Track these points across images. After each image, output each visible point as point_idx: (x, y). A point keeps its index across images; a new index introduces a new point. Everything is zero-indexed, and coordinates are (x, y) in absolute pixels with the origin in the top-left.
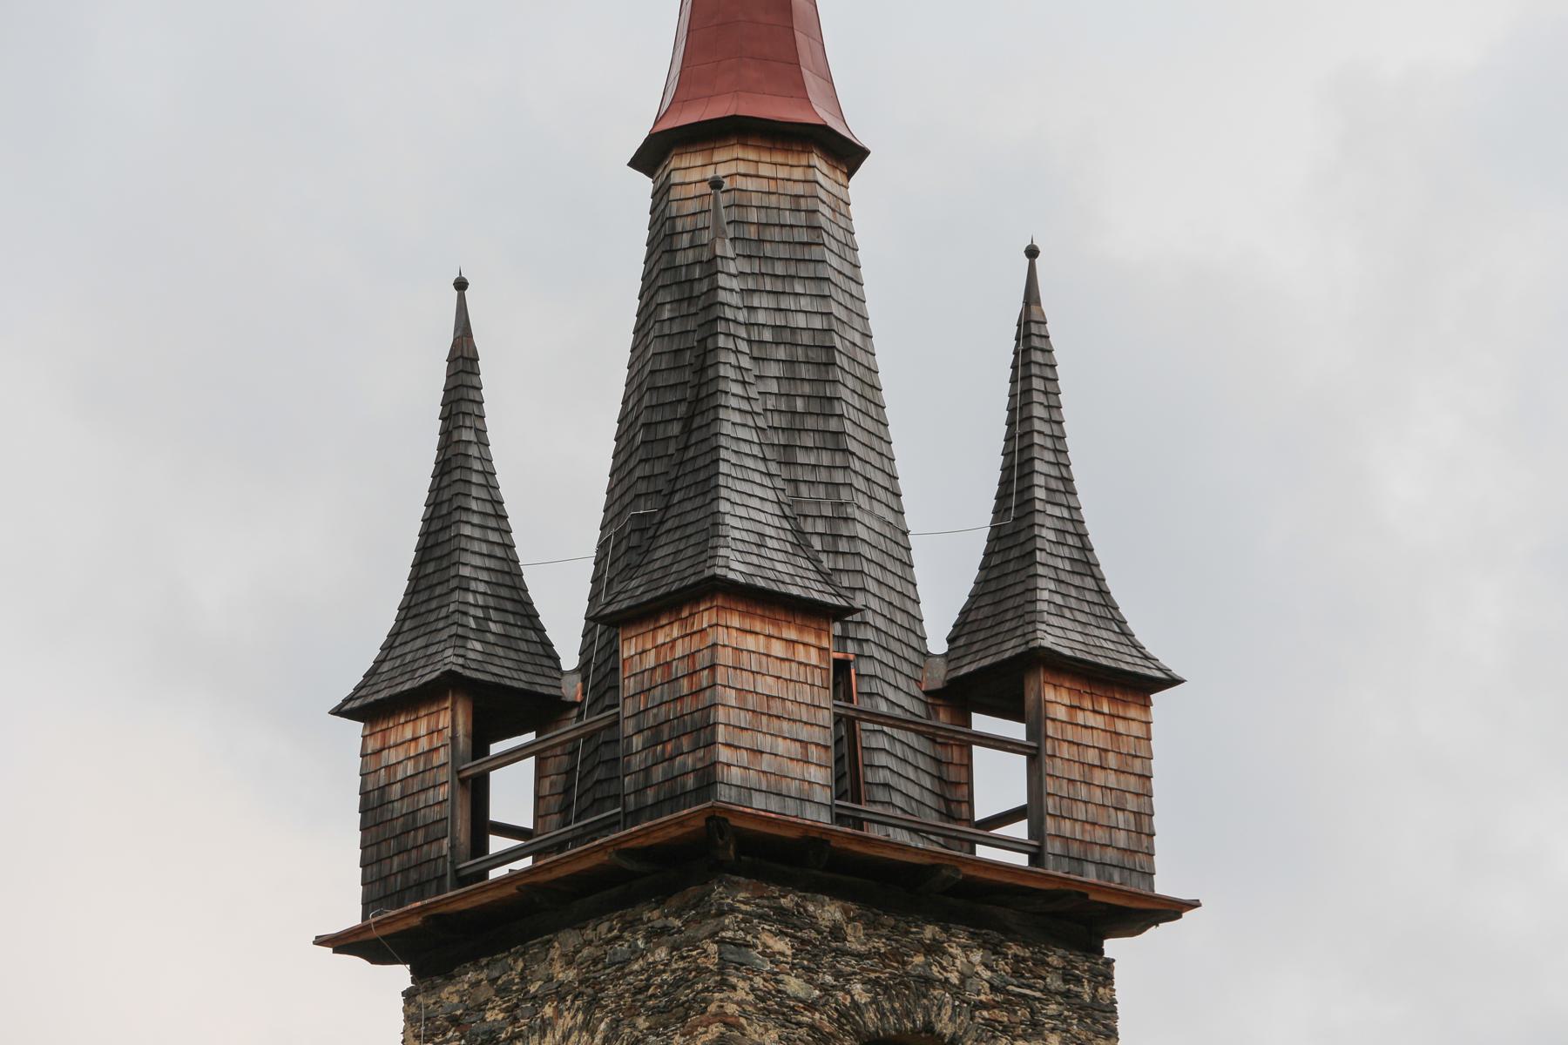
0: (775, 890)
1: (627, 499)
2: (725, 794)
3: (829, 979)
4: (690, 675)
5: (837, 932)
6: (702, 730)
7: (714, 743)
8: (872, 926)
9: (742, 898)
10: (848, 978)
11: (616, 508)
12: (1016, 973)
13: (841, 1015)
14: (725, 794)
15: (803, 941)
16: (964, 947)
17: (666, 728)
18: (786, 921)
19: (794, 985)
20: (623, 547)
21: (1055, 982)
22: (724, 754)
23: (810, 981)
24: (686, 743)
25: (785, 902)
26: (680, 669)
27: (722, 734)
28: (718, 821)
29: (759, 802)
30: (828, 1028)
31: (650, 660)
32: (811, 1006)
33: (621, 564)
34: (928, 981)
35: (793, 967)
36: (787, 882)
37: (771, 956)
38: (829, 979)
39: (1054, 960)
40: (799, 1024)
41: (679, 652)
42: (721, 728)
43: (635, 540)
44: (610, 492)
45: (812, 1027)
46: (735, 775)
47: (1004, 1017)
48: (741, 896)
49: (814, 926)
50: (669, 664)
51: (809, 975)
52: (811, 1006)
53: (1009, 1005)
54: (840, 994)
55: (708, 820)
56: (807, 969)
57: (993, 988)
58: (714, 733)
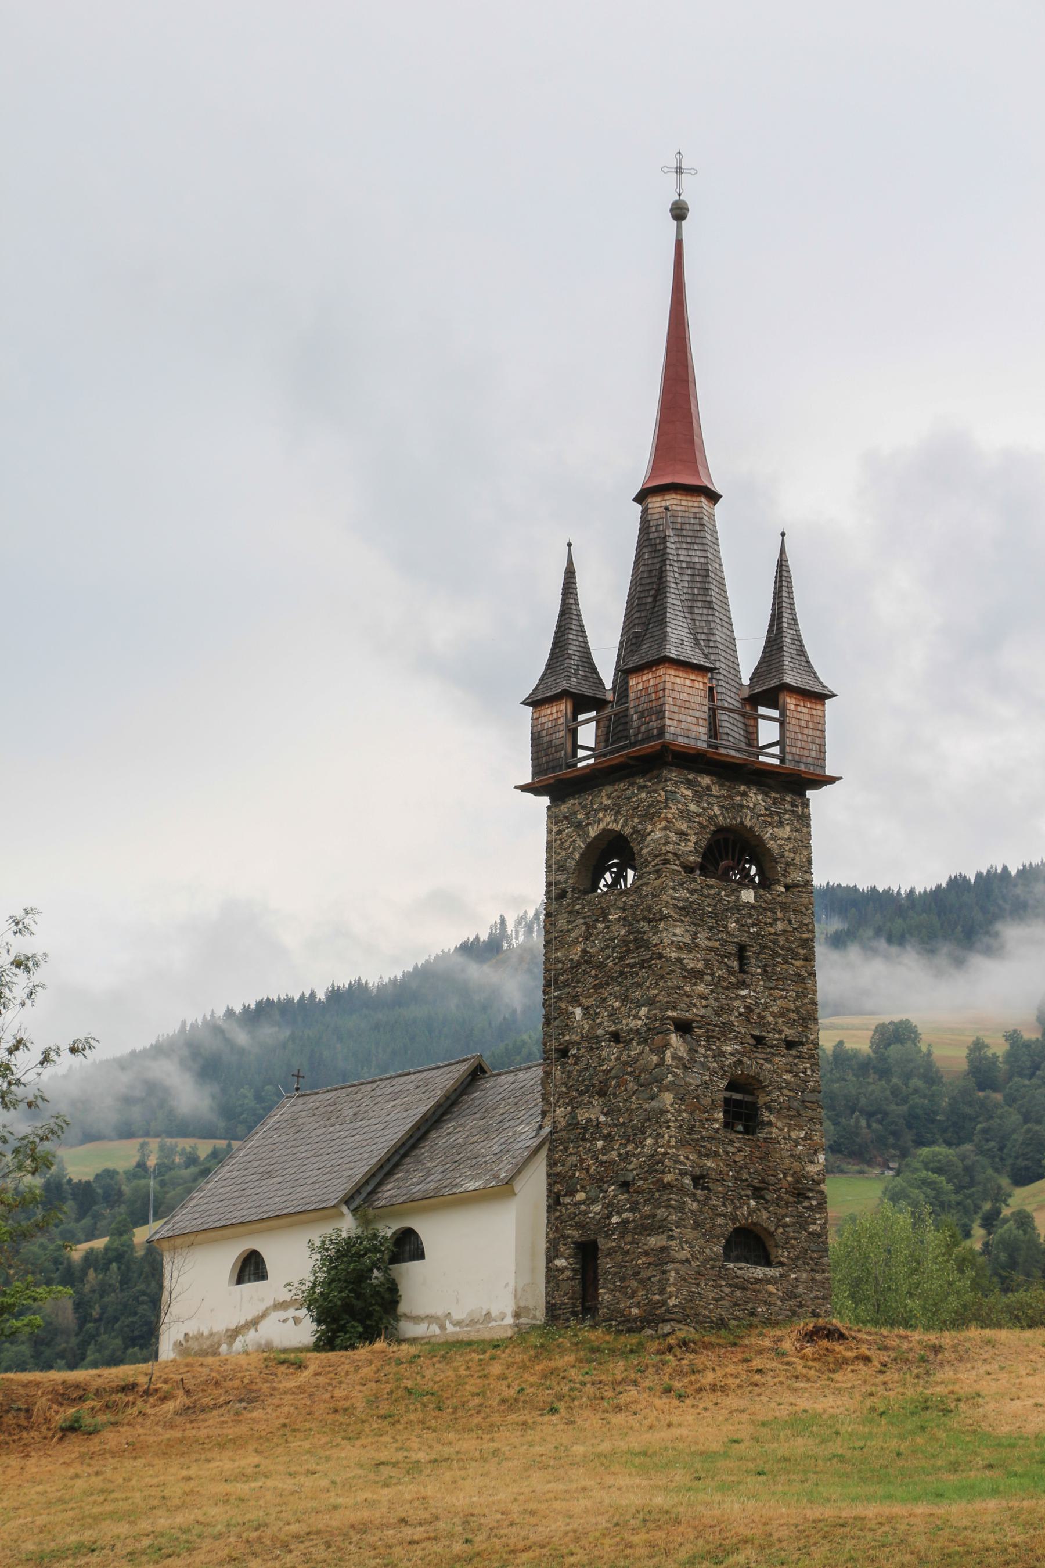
0: (686, 772)
1: (631, 626)
2: (668, 737)
3: (705, 805)
4: (656, 692)
6: (660, 713)
7: (664, 718)
9: (674, 775)
11: (626, 629)
13: (710, 818)
14: (668, 737)
15: (696, 791)
17: (646, 712)
18: (690, 783)
19: (693, 807)
20: (629, 643)
22: (668, 722)
23: (698, 806)
24: (653, 718)
25: (690, 777)
26: (651, 690)
27: (667, 714)
28: (666, 747)
29: (681, 740)
30: (705, 823)
31: (640, 687)
32: (699, 815)
33: (629, 650)
35: (692, 801)
36: (690, 769)
37: (684, 797)
38: (705, 805)
40: (694, 822)
41: (651, 684)
42: (667, 712)
43: (634, 641)
44: (624, 623)
45: (699, 823)
46: (672, 730)
48: (673, 774)
49: (700, 785)
50: (647, 688)
51: (698, 804)
52: (699, 815)
54: (709, 811)
55: (662, 746)
56: (697, 801)
58: (664, 714)
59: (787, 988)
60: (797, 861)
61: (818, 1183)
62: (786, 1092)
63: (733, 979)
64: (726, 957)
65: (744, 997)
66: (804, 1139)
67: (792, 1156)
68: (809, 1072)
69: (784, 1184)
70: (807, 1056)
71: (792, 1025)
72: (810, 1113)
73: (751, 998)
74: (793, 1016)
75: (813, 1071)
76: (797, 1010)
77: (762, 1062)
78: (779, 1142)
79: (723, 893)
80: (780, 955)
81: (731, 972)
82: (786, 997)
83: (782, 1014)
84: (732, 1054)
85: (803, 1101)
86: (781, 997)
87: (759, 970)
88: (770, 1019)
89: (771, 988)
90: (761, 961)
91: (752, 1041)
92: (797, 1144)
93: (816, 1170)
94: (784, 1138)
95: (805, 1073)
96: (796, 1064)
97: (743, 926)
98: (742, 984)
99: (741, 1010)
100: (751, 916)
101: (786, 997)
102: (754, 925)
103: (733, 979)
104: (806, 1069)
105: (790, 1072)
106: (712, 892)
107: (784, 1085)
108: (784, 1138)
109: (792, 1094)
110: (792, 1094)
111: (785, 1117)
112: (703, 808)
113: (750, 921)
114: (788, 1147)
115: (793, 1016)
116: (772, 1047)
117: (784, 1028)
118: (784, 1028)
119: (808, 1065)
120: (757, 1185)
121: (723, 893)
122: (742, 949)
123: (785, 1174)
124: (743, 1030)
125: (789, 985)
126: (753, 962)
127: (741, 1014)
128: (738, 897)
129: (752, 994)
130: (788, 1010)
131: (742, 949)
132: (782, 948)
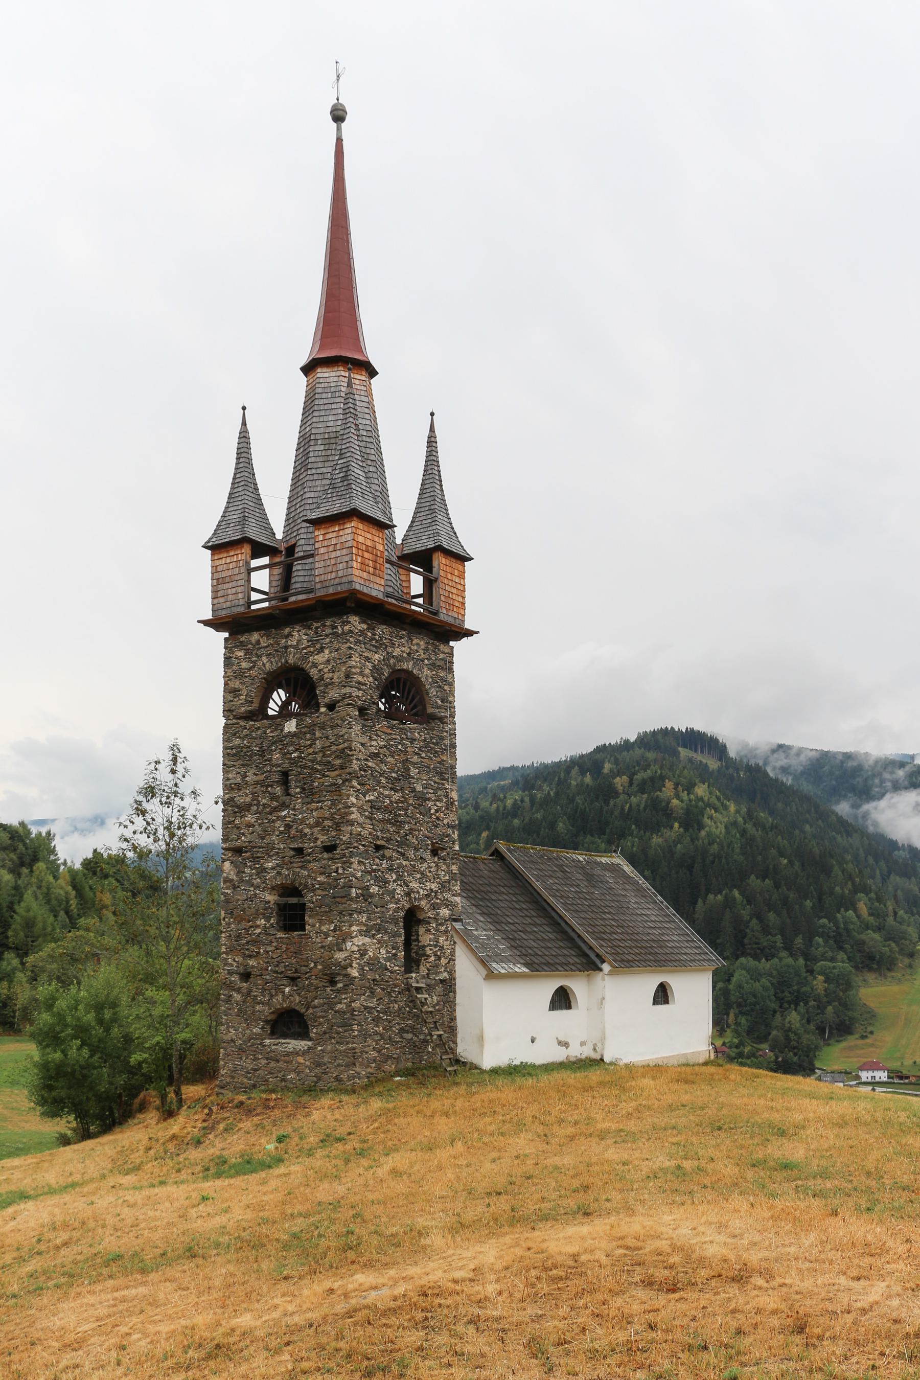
5: (258, 642)
8: (268, 636)
10: (260, 656)
12: (316, 633)
16: (298, 631)
19: (244, 665)
21: (328, 631)
34: (286, 647)
38: (254, 659)
39: (328, 623)
47: (312, 649)
53: (313, 645)
57: (308, 641)
59: (323, 799)
60: (335, 680)
61: (345, 968)
62: (320, 892)
63: (275, 804)
64: (269, 786)
65: (285, 817)
66: (335, 930)
67: (322, 947)
68: (340, 871)
69: (315, 972)
70: (338, 856)
71: (328, 831)
72: (341, 907)
73: (288, 815)
74: (328, 823)
75: (344, 869)
76: (332, 818)
77: (298, 870)
78: (311, 937)
79: (268, 731)
80: (318, 770)
81: (274, 797)
82: (321, 808)
83: (317, 824)
84: (273, 868)
85: (334, 898)
86: (317, 809)
87: (298, 790)
88: (307, 830)
89: (308, 803)
90: (300, 782)
91: (292, 853)
92: (327, 935)
93: (343, 956)
94: (317, 933)
95: (337, 872)
96: (329, 866)
97: (285, 754)
98: (284, 806)
99: (282, 829)
100: (292, 743)
101: (321, 808)
102: (294, 752)
103: (275, 804)
104: (338, 868)
105: (321, 874)
106: (259, 733)
107: (317, 886)
108: (317, 933)
109: (324, 893)
110: (324, 893)
111: (317, 914)
112: (252, 662)
113: (291, 748)
114: (318, 940)
115: (328, 823)
116: (309, 855)
117: (319, 836)
118: (319, 836)
119: (340, 865)
120: (291, 975)
121: (268, 731)
122: (285, 774)
123: (315, 963)
124: (282, 846)
125: (325, 796)
126: (293, 784)
127: (281, 833)
128: (282, 730)
129: (291, 812)
130: (324, 819)
131: (285, 774)
132: (320, 763)
